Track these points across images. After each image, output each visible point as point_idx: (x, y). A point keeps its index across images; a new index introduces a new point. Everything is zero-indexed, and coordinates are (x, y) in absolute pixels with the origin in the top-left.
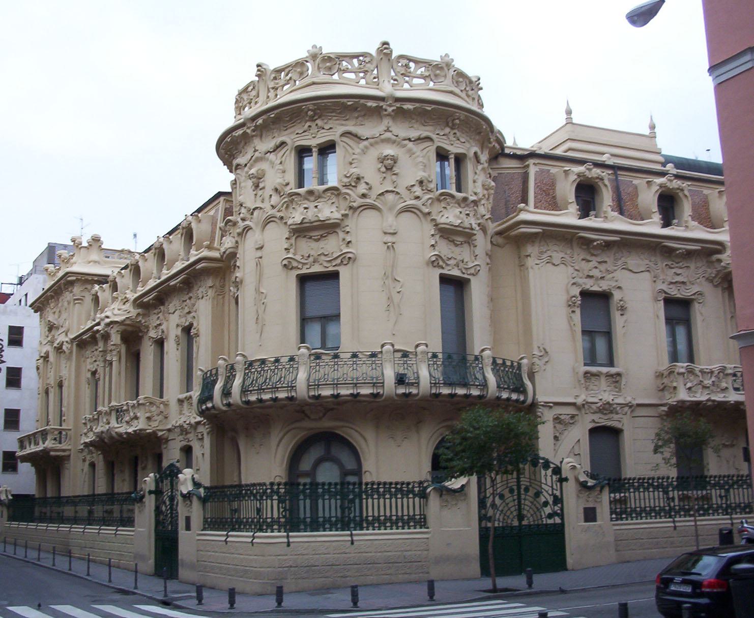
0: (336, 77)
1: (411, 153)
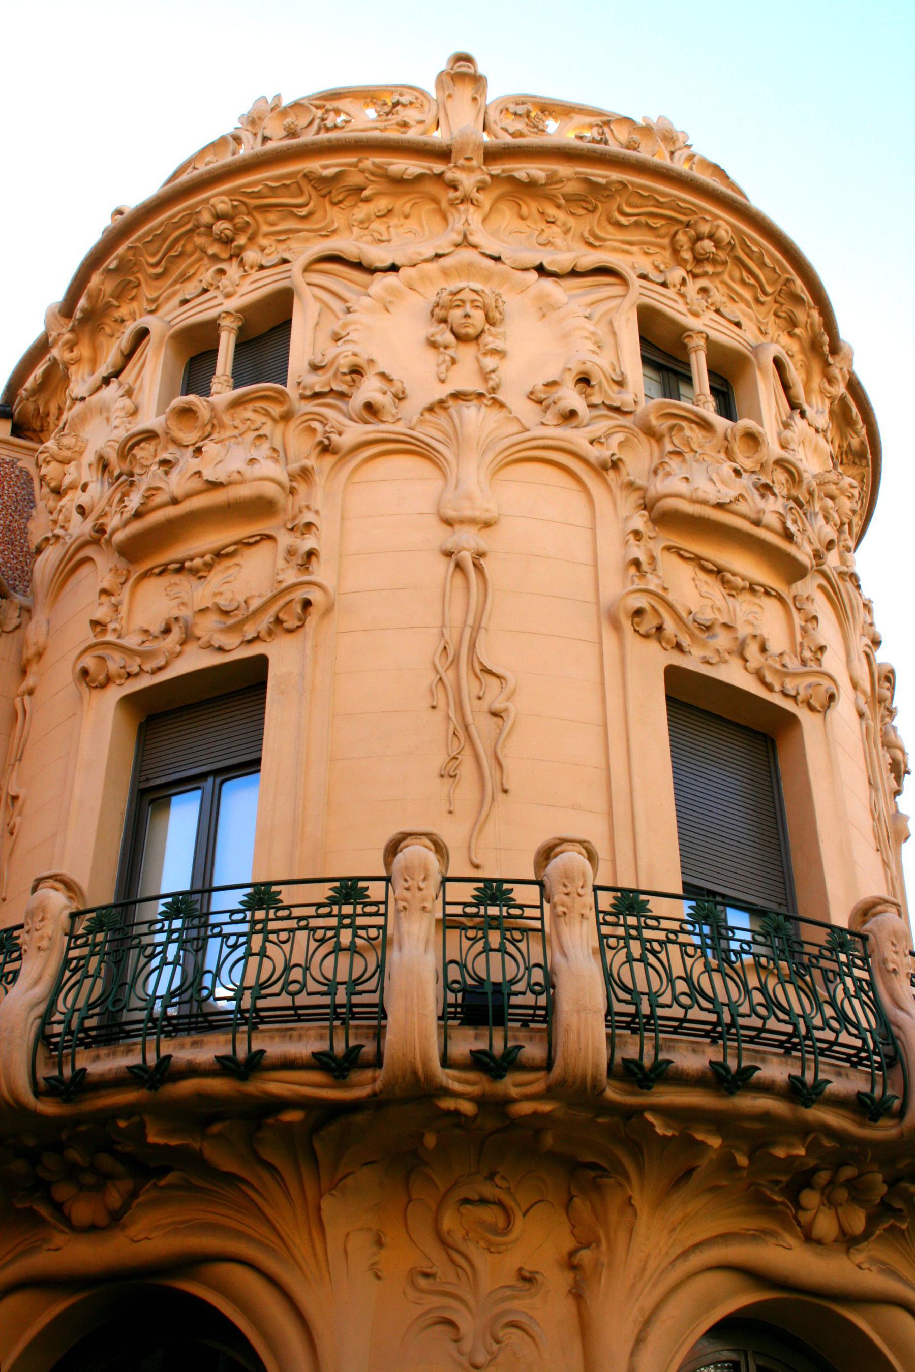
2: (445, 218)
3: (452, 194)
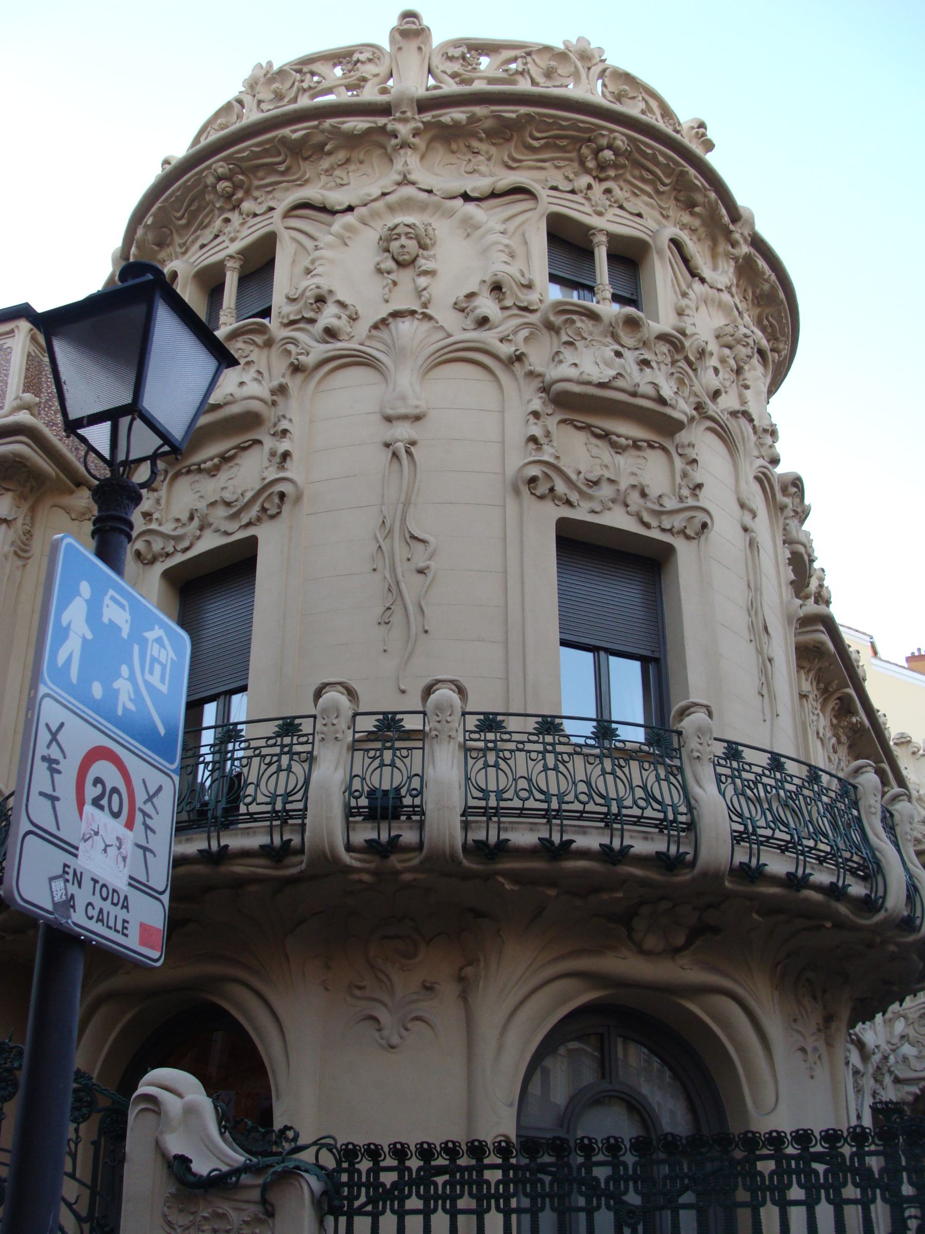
1: (469, 227)
2: (391, 161)
3: (394, 142)
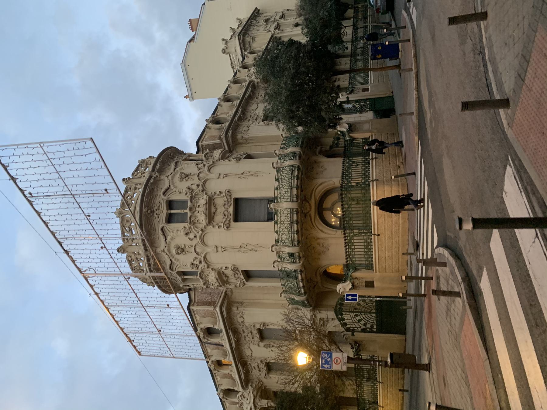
0: (133, 202)
1: (182, 169)
